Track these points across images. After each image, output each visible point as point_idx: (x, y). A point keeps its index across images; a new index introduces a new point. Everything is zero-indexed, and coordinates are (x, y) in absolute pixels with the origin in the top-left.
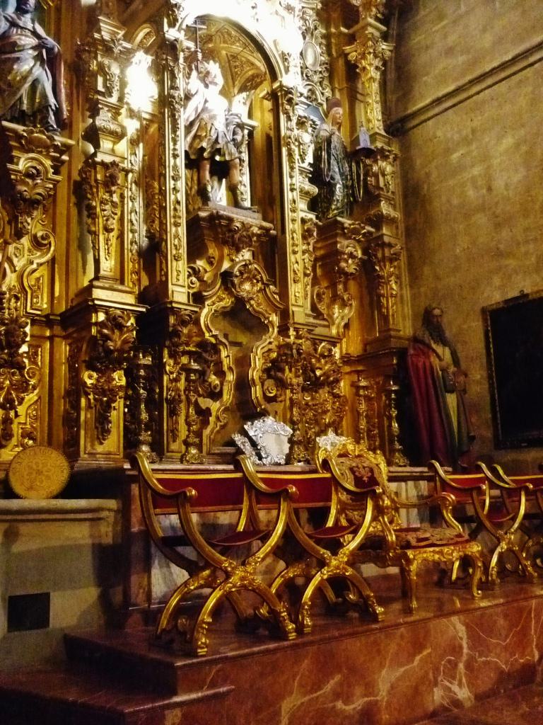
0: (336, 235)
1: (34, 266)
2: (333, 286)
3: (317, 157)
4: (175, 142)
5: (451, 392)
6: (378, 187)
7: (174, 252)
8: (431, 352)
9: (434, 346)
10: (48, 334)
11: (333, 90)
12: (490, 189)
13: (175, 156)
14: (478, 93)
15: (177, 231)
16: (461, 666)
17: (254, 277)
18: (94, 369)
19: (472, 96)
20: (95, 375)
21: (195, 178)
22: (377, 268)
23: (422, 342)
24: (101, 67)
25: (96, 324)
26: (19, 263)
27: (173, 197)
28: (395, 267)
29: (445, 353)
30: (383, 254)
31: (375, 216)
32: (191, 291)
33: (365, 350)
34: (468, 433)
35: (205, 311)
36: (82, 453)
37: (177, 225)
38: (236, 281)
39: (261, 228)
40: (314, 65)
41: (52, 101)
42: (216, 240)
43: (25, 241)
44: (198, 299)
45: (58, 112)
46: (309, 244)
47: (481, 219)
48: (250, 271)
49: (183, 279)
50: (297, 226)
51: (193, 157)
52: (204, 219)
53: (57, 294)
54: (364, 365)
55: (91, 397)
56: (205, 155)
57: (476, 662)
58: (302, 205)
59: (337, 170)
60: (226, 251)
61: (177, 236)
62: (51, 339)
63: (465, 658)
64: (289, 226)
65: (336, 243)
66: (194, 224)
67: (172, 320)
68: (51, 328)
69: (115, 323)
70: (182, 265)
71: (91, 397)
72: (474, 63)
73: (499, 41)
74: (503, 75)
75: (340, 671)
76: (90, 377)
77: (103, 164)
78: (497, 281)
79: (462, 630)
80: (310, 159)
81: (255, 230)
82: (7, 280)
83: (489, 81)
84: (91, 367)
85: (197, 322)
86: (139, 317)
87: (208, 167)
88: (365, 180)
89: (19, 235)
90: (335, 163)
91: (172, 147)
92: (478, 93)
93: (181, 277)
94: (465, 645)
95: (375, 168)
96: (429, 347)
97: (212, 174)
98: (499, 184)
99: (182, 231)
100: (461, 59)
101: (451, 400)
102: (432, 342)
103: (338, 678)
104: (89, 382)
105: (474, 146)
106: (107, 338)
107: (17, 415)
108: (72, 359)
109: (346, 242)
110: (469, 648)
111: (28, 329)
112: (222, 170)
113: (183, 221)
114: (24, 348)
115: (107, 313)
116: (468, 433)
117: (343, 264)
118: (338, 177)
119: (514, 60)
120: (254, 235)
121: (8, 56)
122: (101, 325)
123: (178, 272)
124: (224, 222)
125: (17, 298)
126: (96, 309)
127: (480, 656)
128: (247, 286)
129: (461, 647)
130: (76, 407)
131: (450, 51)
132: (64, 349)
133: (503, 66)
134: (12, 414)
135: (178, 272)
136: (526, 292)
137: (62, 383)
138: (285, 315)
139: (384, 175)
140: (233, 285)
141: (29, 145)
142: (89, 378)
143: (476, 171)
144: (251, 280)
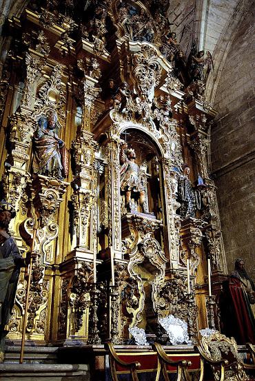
1: (48, 241)
2: (189, 250)
6: (207, 203)
10: (52, 274)
18: (75, 292)
20: (75, 295)
21: (124, 200)
23: (236, 278)
24: (83, 151)
25: (77, 269)
26: (41, 239)
30: (212, 234)
32: (124, 253)
35: (130, 263)
36: (67, 337)
38: (145, 248)
39: (156, 223)
41: (61, 166)
42: (135, 229)
43: (45, 229)
44: (127, 257)
45: (63, 171)
48: (151, 244)
50: (173, 222)
51: (123, 190)
53: (58, 254)
56: (129, 189)
58: (174, 212)
60: (139, 234)
62: (54, 276)
64: (169, 222)
65: (190, 229)
66: (124, 221)
68: (54, 271)
76: (73, 296)
80: (176, 191)
81: (154, 224)
84: (74, 291)
85: (126, 269)
87: (130, 194)
89: (42, 226)
93: (118, 247)
95: (206, 195)
97: (132, 198)
99: (119, 224)
104: (72, 299)
106: (82, 276)
108: (64, 286)
111: (43, 272)
112: (136, 196)
113: (120, 220)
114: (41, 281)
115: (82, 264)
117: (193, 239)
122: (80, 270)
124: (139, 220)
126: (77, 262)
132: (60, 282)
138: (168, 265)
140: (143, 250)
141: (50, 185)
142: (73, 297)
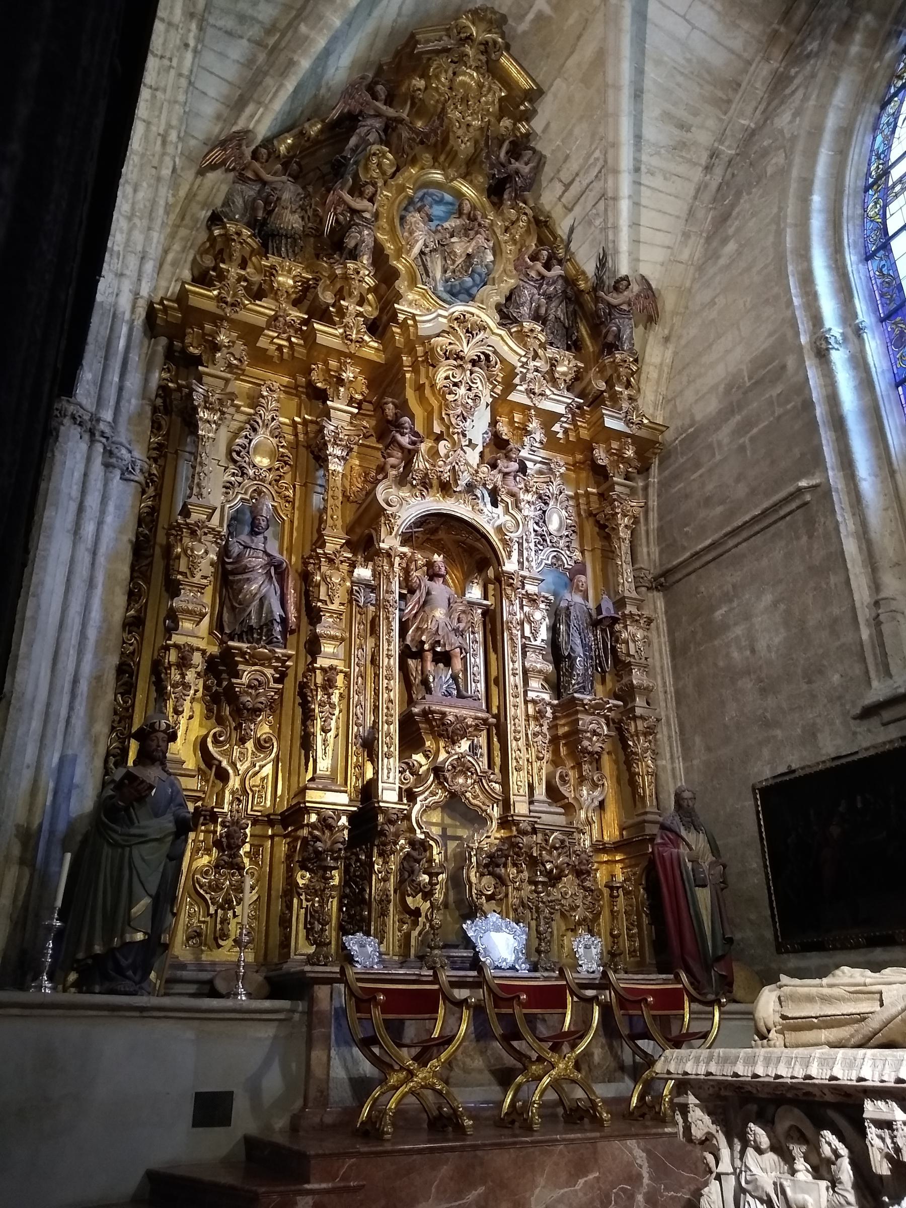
0: (577, 712)
1: (257, 768)
2: (578, 766)
3: (554, 630)
4: (389, 643)
5: (704, 886)
6: (628, 655)
7: (386, 749)
8: (680, 840)
9: (683, 833)
10: (270, 832)
11: (582, 552)
12: (753, 651)
13: (389, 656)
14: (736, 546)
15: (389, 729)
16: (640, 1198)
17: (468, 769)
18: (307, 869)
19: (730, 550)
20: (308, 875)
22: (631, 743)
24: (324, 578)
25: (308, 825)
26: (242, 768)
27: (386, 696)
28: (650, 742)
29: (696, 841)
30: (636, 726)
31: (626, 685)
32: (404, 787)
33: (621, 835)
34: (724, 935)
35: (417, 807)
36: (292, 954)
37: (389, 723)
38: (447, 774)
40: (559, 530)
41: (278, 612)
42: (432, 732)
43: (250, 745)
44: (410, 795)
45: (284, 621)
46: (541, 725)
47: (747, 684)
48: (463, 765)
49: (395, 776)
52: (418, 715)
53: (279, 793)
54: (625, 854)
55: (303, 897)
56: (426, 647)
57: (662, 1196)
59: (579, 641)
60: (442, 744)
61: (388, 734)
62: (272, 837)
63: (645, 1189)
65: (578, 720)
67: (381, 818)
68: (272, 826)
69: (326, 824)
70: (394, 763)
71: (303, 897)
72: (731, 514)
73: (753, 492)
74: (757, 528)
75: (484, 1183)
76: (303, 877)
77: (321, 668)
78: (766, 752)
79: (640, 1156)
80: (543, 634)
82: (231, 783)
83: (745, 534)
84: (304, 867)
85: (408, 817)
86: (352, 817)
88: (614, 649)
89: (242, 741)
90: (576, 635)
91: (386, 647)
92: (736, 546)
93: (391, 775)
94: (646, 1175)
96: (679, 836)
98: (761, 645)
99: (394, 729)
100: (719, 509)
101: (704, 896)
102: (682, 828)
103: (481, 1190)
104: (301, 882)
105: (735, 604)
106: (317, 839)
107: (235, 916)
108: (289, 857)
109: (589, 718)
110: (651, 1178)
111: (248, 831)
113: (396, 720)
114: (247, 848)
115: (318, 814)
116: (724, 935)
117: (586, 743)
118: (579, 650)
119: (765, 513)
120: (469, 726)
121: (240, 577)
122: (313, 826)
123: (389, 770)
124: (437, 716)
125: (239, 801)
126: (308, 811)
127: (666, 1189)
128: (461, 780)
129: (640, 1176)
130: (290, 907)
131: (707, 502)
132: (283, 848)
133: (755, 520)
134: (230, 914)
135: (389, 770)
136: (794, 767)
137: (279, 884)
138: (506, 804)
139: (634, 641)
140: (446, 780)
141: (254, 659)
142: (302, 879)
143: (739, 631)
144: (465, 773)
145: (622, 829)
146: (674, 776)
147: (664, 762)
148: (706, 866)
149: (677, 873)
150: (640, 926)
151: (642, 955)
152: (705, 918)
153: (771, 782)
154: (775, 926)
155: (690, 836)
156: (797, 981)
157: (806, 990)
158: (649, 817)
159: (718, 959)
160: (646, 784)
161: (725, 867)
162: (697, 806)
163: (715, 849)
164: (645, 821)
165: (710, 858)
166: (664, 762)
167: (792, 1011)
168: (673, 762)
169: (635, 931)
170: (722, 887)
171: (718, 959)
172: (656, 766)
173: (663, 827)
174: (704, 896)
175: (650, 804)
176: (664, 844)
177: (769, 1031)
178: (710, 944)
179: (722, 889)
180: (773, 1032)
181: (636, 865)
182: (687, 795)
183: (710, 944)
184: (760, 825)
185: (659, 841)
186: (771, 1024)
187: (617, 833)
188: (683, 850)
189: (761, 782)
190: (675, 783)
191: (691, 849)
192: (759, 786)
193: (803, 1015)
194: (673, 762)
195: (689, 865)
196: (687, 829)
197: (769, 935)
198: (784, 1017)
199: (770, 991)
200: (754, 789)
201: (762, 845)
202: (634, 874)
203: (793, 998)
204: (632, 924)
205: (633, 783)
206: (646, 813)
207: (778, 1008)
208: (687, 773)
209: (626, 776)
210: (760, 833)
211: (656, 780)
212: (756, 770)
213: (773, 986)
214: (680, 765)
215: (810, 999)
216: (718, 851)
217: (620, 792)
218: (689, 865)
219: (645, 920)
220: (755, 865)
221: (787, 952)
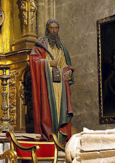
5: (59, 82)
8: (46, 53)
9: (49, 49)
33: (11, 49)
34: (67, 111)
54: (12, 61)
96: (46, 50)
101: (58, 88)
102: (49, 46)
116: (67, 111)
145: (11, 46)
146: (49, 14)
147: (43, 4)
148: (61, 70)
149: (43, 73)
150: (18, 107)
151: (18, 124)
152: (57, 101)
153: (109, 20)
154: (100, 108)
155: (53, 51)
156: (92, 131)
157: (95, 136)
158: (30, 38)
159: (62, 126)
160: (29, 18)
161: (73, 71)
162: (60, 33)
163: (68, 60)
164: (26, 41)
165: (65, 65)
166: (43, 4)
167: (87, 147)
168: (49, 4)
169: (15, 108)
170: (70, 82)
171: (62, 126)
172: (37, 6)
173: (37, 45)
174: (58, 88)
175: (31, 31)
176: (37, 55)
177: (73, 159)
178: (58, 116)
179: (70, 85)
180: (75, 160)
181: (18, 68)
182: (53, 25)
183: (58, 116)
184: (98, 47)
185: (33, 53)
186: (74, 155)
187: (8, 48)
188: (48, 59)
189: (102, 19)
190: (49, 18)
191: (53, 59)
192: (101, 22)
193: (92, 149)
194: (49, 4)
195: (51, 69)
196: (52, 46)
197: (96, 113)
198: (82, 151)
199: (76, 137)
200: (97, 24)
201: (99, 59)
202: (17, 74)
203: (87, 140)
204: (13, 105)
205: (21, 16)
206: (27, 36)
207: (79, 146)
208: (57, 12)
209: (18, 12)
210: (98, 51)
211: (36, 15)
212: (100, 11)
213: (79, 134)
214: (53, 6)
215: (97, 141)
216: (70, 61)
217: (12, 22)
218: (51, 69)
219: (22, 102)
220: (93, 71)
221: (106, 123)
